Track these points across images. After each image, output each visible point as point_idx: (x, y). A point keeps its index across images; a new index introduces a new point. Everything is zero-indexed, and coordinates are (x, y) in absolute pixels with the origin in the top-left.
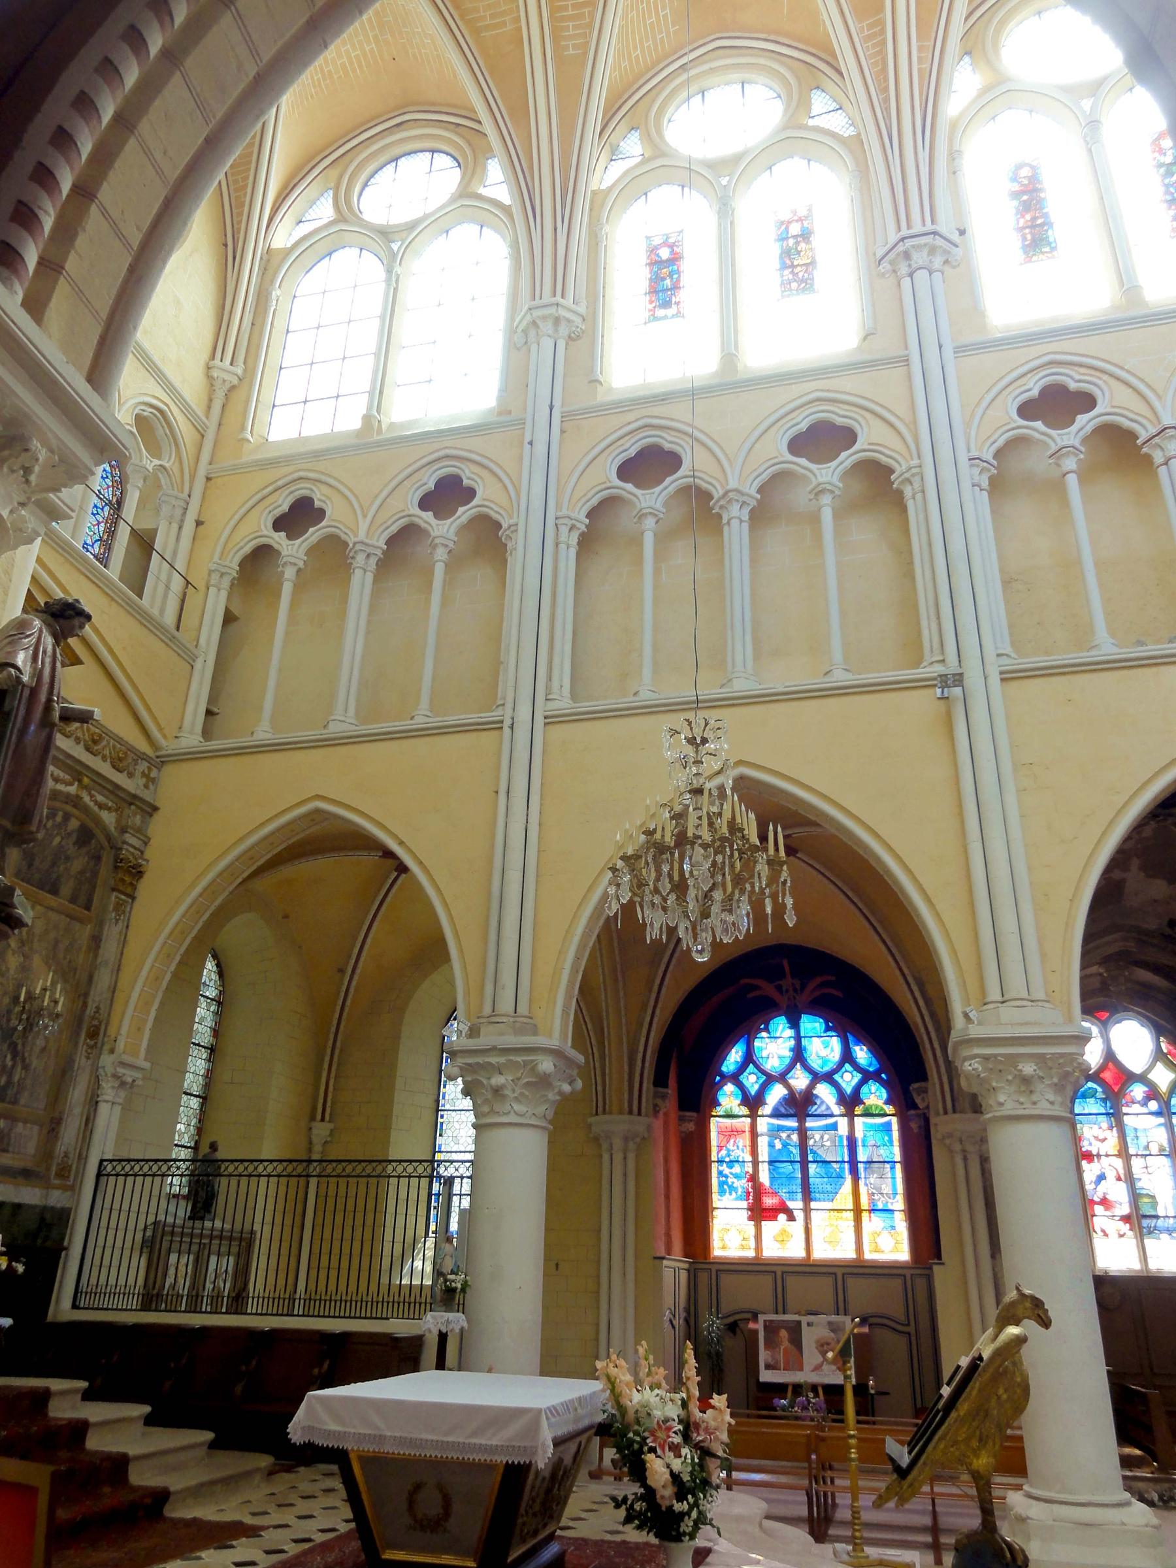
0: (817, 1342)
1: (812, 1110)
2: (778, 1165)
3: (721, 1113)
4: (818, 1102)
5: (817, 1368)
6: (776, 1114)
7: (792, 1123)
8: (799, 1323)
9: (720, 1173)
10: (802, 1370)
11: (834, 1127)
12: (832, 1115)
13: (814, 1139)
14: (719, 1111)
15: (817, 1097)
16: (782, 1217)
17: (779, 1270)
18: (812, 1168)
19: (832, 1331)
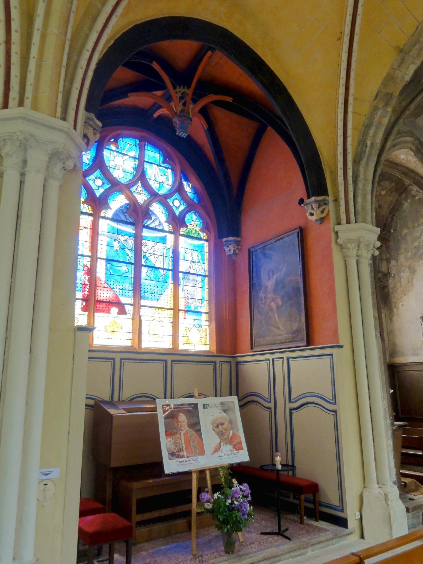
1: (148, 223)
2: (114, 263)
4: (153, 217)
5: (217, 449)
6: (115, 219)
7: (130, 229)
8: (196, 406)
10: (202, 452)
11: (163, 240)
12: (163, 231)
13: (148, 246)
15: (153, 213)
16: (114, 310)
17: (118, 357)
18: (144, 270)
19: (225, 411)
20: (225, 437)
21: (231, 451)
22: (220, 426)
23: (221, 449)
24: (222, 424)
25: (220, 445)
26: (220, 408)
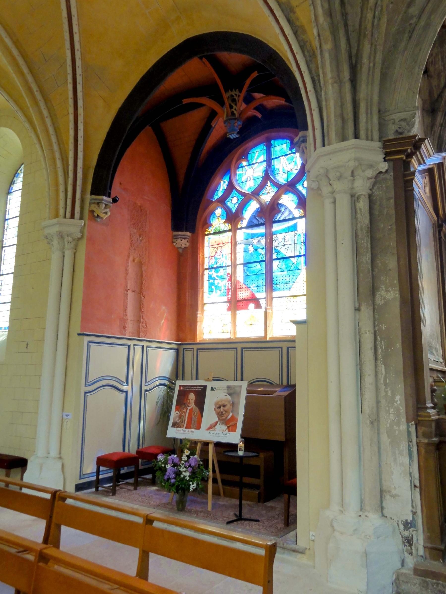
0: (216, 404)
1: (279, 217)
2: (250, 265)
3: (213, 232)
4: (282, 210)
5: (212, 427)
6: (251, 225)
7: (261, 230)
8: (205, 387)
9: (210, 277)
10: (199, 427)
11: (294, 228)
12: (293, 219)
13: (279, 240)
14: (212, 230)
15: (282, 205)
16: (252, 306)
17: (239, 346)
18: (275, 264)
19: (230, 394)
20: (224, 418)
21: (223, 431)
22: (222, 408)
23: (216, 427)
24: (224, 406)
25: (216, 424)
26: (226, 391)
